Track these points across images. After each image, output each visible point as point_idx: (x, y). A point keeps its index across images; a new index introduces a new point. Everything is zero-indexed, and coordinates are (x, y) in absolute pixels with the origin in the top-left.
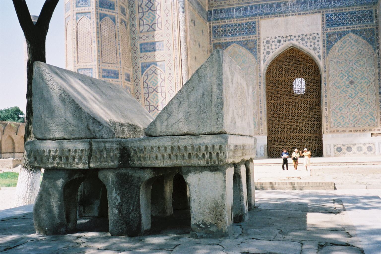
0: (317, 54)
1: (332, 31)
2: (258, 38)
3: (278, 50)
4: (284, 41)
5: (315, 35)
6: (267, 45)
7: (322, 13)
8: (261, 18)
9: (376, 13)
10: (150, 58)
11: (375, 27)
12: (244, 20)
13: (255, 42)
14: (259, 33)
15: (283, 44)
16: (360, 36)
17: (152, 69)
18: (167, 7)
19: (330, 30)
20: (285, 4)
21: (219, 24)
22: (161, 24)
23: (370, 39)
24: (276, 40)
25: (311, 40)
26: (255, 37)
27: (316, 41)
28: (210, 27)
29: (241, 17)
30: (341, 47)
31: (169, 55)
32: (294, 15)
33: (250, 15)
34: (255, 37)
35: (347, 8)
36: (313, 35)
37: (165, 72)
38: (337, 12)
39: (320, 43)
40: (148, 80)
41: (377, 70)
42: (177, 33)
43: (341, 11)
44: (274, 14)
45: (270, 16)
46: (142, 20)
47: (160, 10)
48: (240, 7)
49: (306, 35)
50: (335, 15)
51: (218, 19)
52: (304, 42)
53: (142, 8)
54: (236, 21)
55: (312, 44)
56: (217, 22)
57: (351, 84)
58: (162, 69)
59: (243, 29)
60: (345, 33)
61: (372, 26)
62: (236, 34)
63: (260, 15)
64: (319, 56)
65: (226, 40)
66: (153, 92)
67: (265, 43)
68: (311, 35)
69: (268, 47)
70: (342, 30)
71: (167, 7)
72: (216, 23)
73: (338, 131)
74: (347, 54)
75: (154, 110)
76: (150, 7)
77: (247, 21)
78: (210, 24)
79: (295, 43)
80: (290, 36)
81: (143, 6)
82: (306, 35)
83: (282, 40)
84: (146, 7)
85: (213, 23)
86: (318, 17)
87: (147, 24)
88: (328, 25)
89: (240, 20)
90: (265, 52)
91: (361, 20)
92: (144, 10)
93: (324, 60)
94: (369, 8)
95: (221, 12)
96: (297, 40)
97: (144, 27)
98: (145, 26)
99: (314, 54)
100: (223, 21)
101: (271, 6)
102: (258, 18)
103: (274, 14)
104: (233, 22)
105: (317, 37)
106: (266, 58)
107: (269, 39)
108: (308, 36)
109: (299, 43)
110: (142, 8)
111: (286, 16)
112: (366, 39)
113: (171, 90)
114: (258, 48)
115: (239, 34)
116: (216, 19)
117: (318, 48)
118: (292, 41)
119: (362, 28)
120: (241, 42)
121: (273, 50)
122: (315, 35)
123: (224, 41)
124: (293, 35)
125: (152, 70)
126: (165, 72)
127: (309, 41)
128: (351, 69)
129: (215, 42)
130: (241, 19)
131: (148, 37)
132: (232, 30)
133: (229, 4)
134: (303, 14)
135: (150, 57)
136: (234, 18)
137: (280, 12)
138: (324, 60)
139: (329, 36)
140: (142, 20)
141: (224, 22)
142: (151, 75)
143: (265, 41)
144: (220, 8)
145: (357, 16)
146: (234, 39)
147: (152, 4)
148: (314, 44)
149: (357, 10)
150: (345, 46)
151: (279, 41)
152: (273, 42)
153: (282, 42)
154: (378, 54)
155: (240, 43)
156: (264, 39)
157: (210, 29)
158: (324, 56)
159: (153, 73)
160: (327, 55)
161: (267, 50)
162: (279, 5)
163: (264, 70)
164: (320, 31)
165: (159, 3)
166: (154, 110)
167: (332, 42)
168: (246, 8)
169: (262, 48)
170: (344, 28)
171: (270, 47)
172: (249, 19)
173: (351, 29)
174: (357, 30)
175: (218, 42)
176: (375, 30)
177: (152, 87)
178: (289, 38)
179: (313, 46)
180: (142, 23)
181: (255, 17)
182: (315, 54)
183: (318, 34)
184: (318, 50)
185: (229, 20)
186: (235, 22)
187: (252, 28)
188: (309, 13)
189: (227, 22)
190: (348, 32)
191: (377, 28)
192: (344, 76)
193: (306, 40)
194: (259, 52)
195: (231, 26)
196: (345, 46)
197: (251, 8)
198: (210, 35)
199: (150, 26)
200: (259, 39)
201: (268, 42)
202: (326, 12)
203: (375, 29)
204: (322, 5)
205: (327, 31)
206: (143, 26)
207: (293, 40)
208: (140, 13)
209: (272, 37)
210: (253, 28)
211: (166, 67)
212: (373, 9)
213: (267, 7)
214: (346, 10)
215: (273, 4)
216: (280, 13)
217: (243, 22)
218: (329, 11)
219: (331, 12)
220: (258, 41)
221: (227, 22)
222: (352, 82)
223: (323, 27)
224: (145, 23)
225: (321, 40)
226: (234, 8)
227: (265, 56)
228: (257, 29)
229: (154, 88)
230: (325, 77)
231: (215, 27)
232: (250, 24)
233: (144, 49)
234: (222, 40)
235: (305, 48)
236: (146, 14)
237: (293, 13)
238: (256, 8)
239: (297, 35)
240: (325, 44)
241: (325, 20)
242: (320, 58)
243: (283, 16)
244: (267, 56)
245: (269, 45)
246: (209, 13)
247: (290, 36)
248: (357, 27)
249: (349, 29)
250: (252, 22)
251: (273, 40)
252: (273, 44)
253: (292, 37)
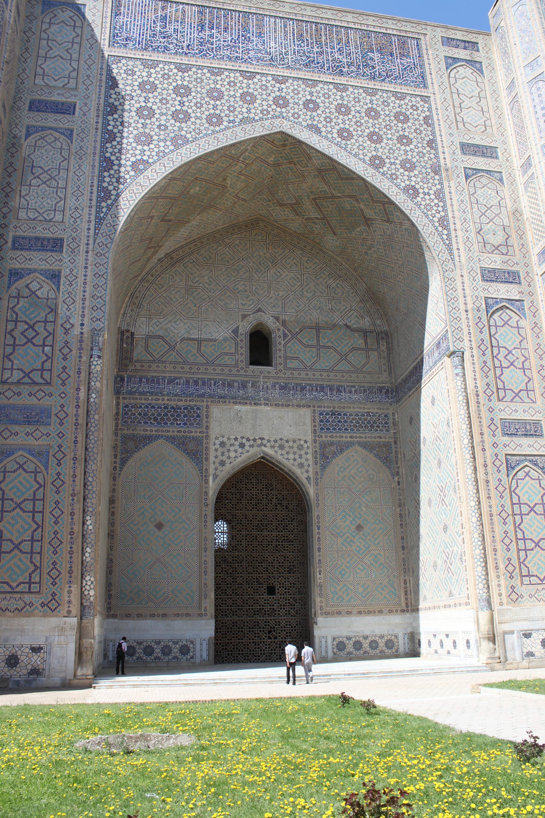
0: (305, 475)
1: (328, 439)
2: (205, 434)
3: (239, 460)
4: (250, 446)
5: (302, 442)
6: (221, 450)
7: (312, 408)
8: (212, 402)
9: (394, 419)
10: (18, 437)
11: (392, 440)
12: (182, 400)
13: (198, 441)
14: (207, 427)
15: (248, 451)
16: (371, 452)
17: (18, 460)
18: (66, 343)
19: (326, 438)
20: (253, 385)
21: (135, 401)
22: (49, 372)
23: (385, 459)
24: (237, 443)
25: (295, 449)
26: (200, 432)
27: (303, 452)
28: (118, 404)
29: (177, 395)
30: (342, 467)
31: (61, 435)
32: (267, 404)
33: (193, 394)
34: (200, 432)
35: (352, 406)
36: (298, 442)
37: (47, 469)
38: (336, 409)
39: (310, 456)
40: (6, 482)
41: (398, 510)
42: (82, 394)
43: (342, 410)
44: (236, 400)
45: (227, 401)
46: (10, 360)
47: (52, 346)
48: (177, 378)
49: (287, 441)
50: (333, 414)
51: (135, 392)
52: (284, 452)
53: (12, 336)
54: (168, 400)
55: (297, 456)
56: (132, 396)
57: (359, 531)
58: (40, 462)
59: (179, 416)
60: (349, 445)
61: (389, 438)
62: (166, 424)
63: (211, 396)
64: (308, 478)
65: (147, 430)
66: (13, 510)
67: (217, 446)
68: (294, 441)
69: (223, 454)
70: (344, 439)
71: (66, 343)
72: (130, 399)
73: (339, 613)
74: (352, 479)
75: (12, 550)
76: (30, 337)
77: (188, 403)
78: (118, 398)
79: (269, 451)
80: (260, 438)
81: (16, 333)
82: (287, 441)
83: (247, 444)
84: (22, 337)
85: (123, 398)
86: (306, 414)
87: (18, 369)
89: (174, 400)
90: (217, 461)
91: (372, 427)
92: (17, 343)
93: (317, 485)
94: (383, 409)
95: (141, 381)
96: (273, 447)
97: (12, 374)
98: (14, 372)
99: (301, 474)
100: (143, 397)
101: (230, 385)
102: (207, 401)
103: (235, 398)
104: (164, 401)
105: (305, 446)
106: (218, 473)
107: (225, 439)
108: (291, 443)
109: (276, 452)
110: (12, 336)
111: (255, 404)
112: (380, 458)
113: (57, 510)
114: (204, 452)
115: (172, 424)
116: (131, 393)
117: (306, 464)
118: (263, 448)
119: (373, 440)
120: (173, 438)
121: (232, 460)
122: (302, 442)
123: (142, 433)
124: (267, 438)
125: (18, 463)
126: (47, 469)
127: (291, 451)
128: (358, 505)
129: (125, 432)
130: (177, 398)
131: (19, 394)
132: (159, 415)
133: (156, 369)
134: (282, 405)
135: (17, 434)
136: (164, 395)
137: (244, 396)
138: (317, 485)
140: (10, 360)
141: (145, 399)
142: (15, 471)
143: (217, 442)
144: (139, 374)
145: (366, 419)
146: (162, 431)
147: (35, 333)
149: (366, 411)
150: (349, 466)
151: (242, 446)
152: (232, 445)
153: (247, 448)
154: (399, 482)
155: (172, 439)
156: (217, 438)
157: (118, 409)
158: (317, 479)
159: (18, 469)
160: (321, 478)
161: (221, 458)
162: (244, 386)
163: (214, 493)
164: (310, 438)
165: (50, 334)
166: (12, 550)
168: (188, 382)
169: (212, 454)
170: (346, 437)
171: (226, 454)
172: (190, 401)
173: (358, 439)
174: (366, 443)
175: (131, 432)
176: (393, 446)
177: (12, 500)
178: (259, 442)
179: (299, 461)
180: (8, 365)
181: (202, 399)
182: (302, 473)
183: (306, 442)
184: (306, 468)
185: (154, 398)
186: (166, 402)
187: (194, 416)
188: (293, 406)
189: (151, 400)
190: (352, 444)
191: (395, 443)
192: (347, 517)
193: (287, 449)
194: (207, 459)
195: (158, 408)
196: (349, 466)
197: (196, 383)
198: (117, 419)
199: (25, 373)
200: (207, 437)
201: (222, 444)
203: (393, 443)
204: (312, 396)
205: (321, 439)
206: (10, 372)
207: (265, 446)
208: (7, 345)
209: (231, 437)
210: (197, 417)
211: (51, 458)
212: (390, 412)
213: (223, 384)
214: (350, 408)
215: (234, 381)
216: (244, 399)
217: (180, 403)
218: (324, 407)
219: (326, 409)
220: (205, 441)
221: (151, 400)
222: (359, 528)
223: (315, 430)
224: (15, 367)
225: (310, 451)
226: (165, 377)
227: (216, 469)
228: (205, 420)
229: (18, 502)
230: (318, 515)
231: (127, 406)
232: (192, 408)
233: (7, 416)
234: (140, 430)
235: (285, 461)
236: (20, 351)
237: (267, 402)
238: (204, 384)
239: (272, 439)
241: (318, 420)
243: (250, 404)
244: (220, 468)
245: (225, 450)
246: (119, 379)
247: (260, 438)
248: (370, 436)
249: (354, 439)
250: (195, 405)
251: (232, 441)
252: (232, 448)
253: (265, 442)
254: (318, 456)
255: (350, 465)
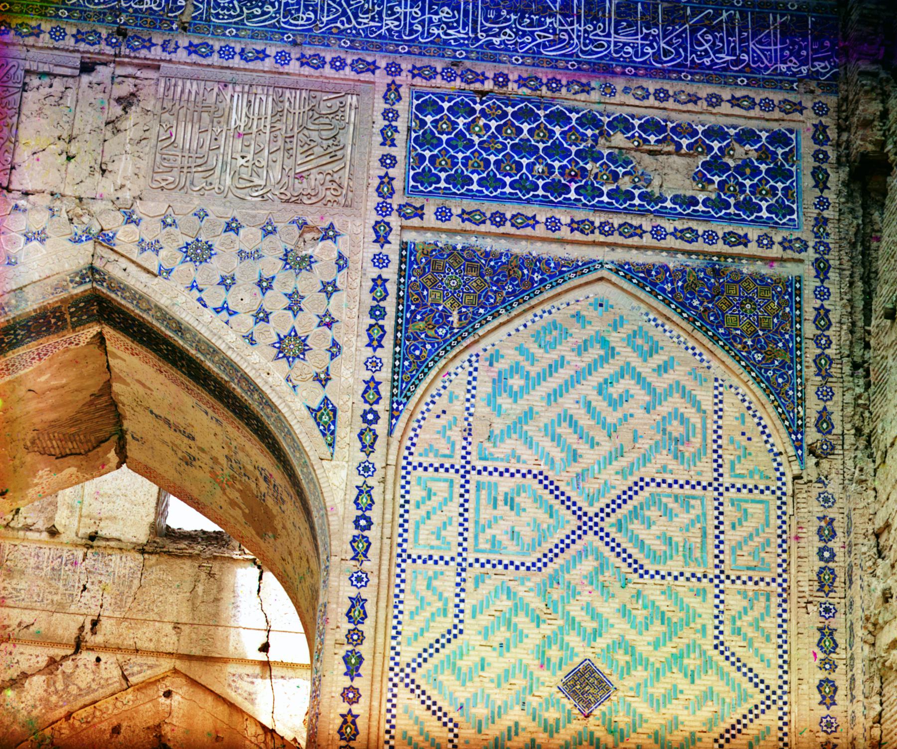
30: (515, 369)
55: (275, 301)
74: (564, 430)
88: (423, 178)
93: (368, 448)
138: (368, 448)
139: (421, 265)
148: (295, 304)
150: (552, 369)
158: (369, 418)
160: (394, 415)
167: (445, 315)
179: (282, 321)
192: (522, 621)
196: (552, 369)
202: (416, 72)
240: (389, 323)
242: (328, 431)
254: (390, 305)
255: (562, 362)
